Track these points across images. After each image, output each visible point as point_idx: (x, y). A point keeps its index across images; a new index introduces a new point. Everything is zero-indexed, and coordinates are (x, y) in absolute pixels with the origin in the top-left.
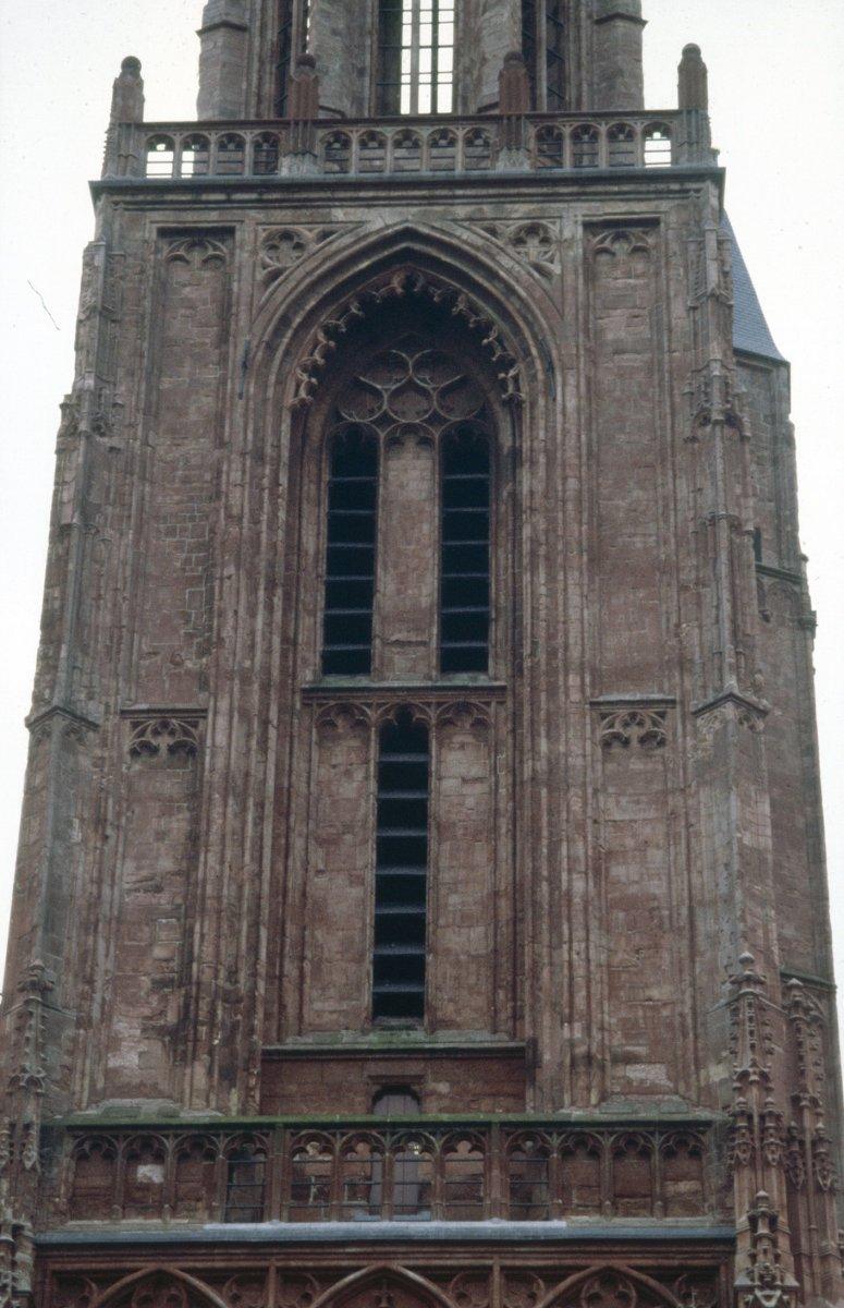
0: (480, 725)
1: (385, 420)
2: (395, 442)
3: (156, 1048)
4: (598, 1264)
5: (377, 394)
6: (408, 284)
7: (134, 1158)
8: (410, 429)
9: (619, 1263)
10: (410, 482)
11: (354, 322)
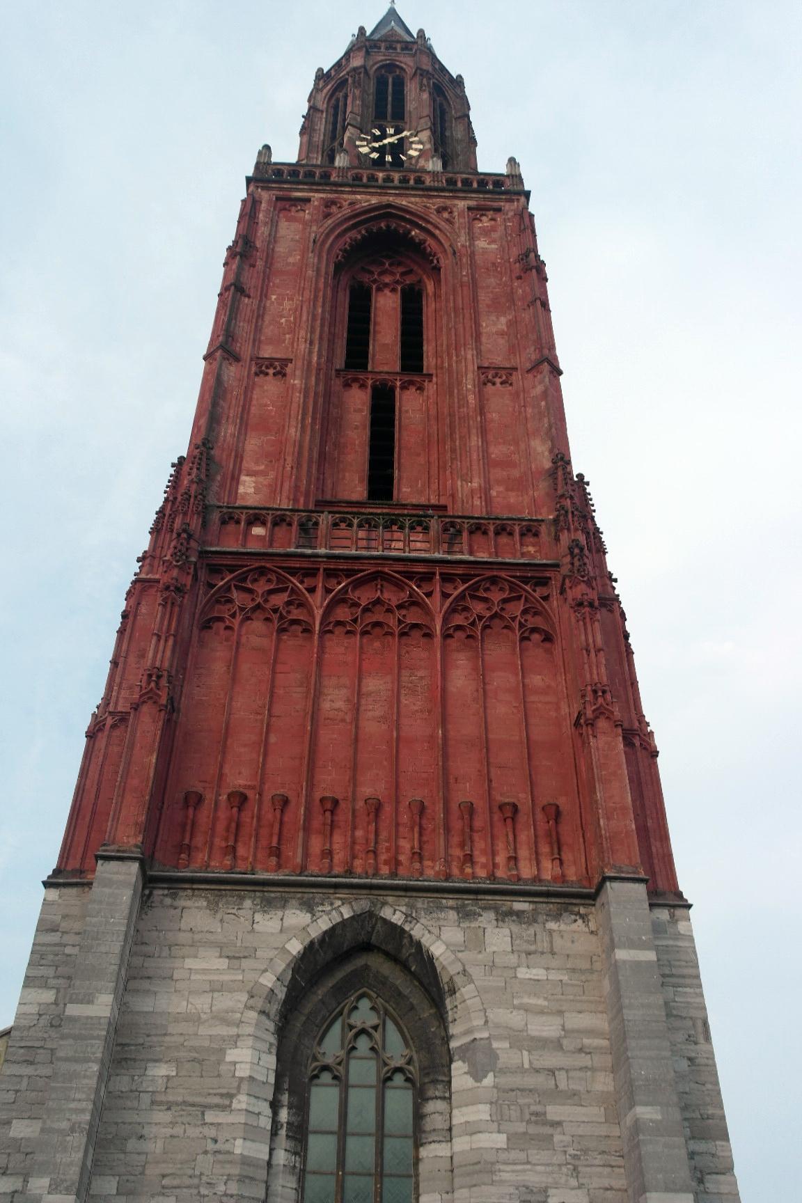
0: (420, 389)
1: (375, 281)
2: (379, 289)
4: (489, 574)
5: (372, 273)
6: (388, 227)
7: (251, 523)
8: (386, 285)
9: (503, 574)
10: (387, 306)
11: (363, 237)
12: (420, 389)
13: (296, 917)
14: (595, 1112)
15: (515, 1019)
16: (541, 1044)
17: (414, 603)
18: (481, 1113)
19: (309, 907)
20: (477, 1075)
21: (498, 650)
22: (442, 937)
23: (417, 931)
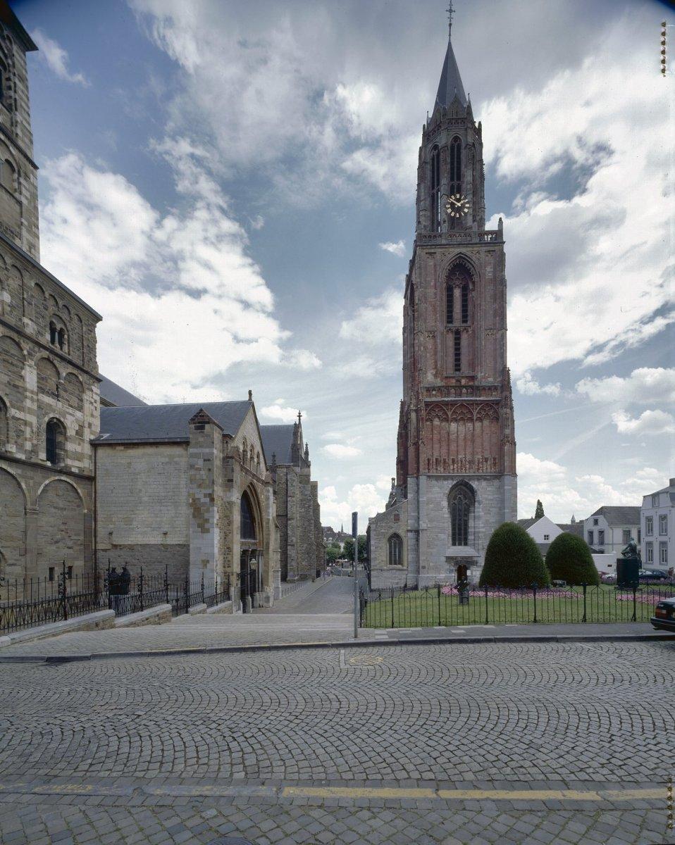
3: (433, 377)
12: (467, 331)
13: (450, 482)
14: (497, 510)
15: (486, 496)
16: (490, 500)
17: (470, 411)
18: (481, 510)
19: (452, 479)
20: (479, 504)
21: (486, 422)
22: (475, 484)
23: (470, 483)
